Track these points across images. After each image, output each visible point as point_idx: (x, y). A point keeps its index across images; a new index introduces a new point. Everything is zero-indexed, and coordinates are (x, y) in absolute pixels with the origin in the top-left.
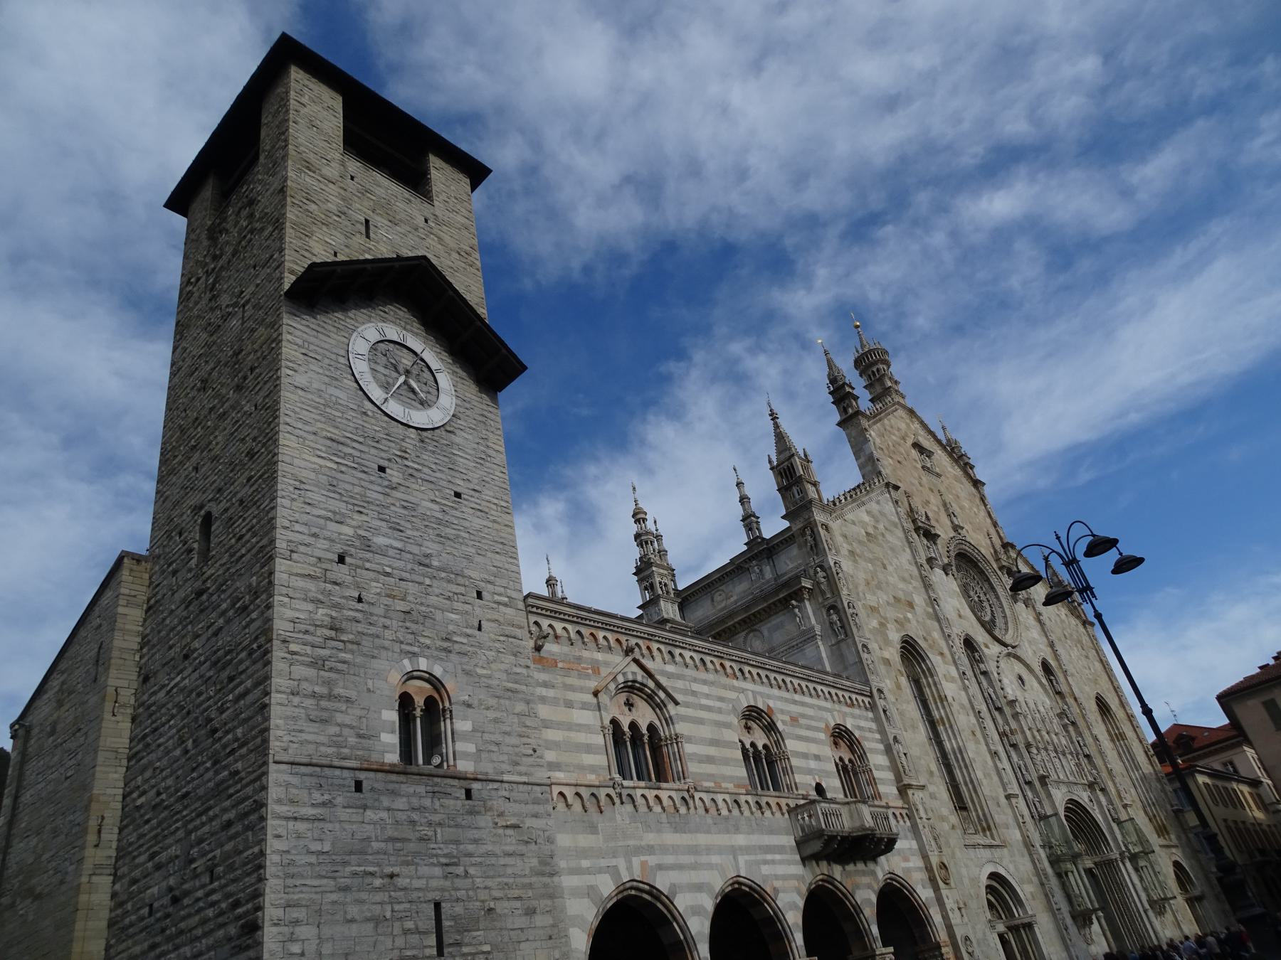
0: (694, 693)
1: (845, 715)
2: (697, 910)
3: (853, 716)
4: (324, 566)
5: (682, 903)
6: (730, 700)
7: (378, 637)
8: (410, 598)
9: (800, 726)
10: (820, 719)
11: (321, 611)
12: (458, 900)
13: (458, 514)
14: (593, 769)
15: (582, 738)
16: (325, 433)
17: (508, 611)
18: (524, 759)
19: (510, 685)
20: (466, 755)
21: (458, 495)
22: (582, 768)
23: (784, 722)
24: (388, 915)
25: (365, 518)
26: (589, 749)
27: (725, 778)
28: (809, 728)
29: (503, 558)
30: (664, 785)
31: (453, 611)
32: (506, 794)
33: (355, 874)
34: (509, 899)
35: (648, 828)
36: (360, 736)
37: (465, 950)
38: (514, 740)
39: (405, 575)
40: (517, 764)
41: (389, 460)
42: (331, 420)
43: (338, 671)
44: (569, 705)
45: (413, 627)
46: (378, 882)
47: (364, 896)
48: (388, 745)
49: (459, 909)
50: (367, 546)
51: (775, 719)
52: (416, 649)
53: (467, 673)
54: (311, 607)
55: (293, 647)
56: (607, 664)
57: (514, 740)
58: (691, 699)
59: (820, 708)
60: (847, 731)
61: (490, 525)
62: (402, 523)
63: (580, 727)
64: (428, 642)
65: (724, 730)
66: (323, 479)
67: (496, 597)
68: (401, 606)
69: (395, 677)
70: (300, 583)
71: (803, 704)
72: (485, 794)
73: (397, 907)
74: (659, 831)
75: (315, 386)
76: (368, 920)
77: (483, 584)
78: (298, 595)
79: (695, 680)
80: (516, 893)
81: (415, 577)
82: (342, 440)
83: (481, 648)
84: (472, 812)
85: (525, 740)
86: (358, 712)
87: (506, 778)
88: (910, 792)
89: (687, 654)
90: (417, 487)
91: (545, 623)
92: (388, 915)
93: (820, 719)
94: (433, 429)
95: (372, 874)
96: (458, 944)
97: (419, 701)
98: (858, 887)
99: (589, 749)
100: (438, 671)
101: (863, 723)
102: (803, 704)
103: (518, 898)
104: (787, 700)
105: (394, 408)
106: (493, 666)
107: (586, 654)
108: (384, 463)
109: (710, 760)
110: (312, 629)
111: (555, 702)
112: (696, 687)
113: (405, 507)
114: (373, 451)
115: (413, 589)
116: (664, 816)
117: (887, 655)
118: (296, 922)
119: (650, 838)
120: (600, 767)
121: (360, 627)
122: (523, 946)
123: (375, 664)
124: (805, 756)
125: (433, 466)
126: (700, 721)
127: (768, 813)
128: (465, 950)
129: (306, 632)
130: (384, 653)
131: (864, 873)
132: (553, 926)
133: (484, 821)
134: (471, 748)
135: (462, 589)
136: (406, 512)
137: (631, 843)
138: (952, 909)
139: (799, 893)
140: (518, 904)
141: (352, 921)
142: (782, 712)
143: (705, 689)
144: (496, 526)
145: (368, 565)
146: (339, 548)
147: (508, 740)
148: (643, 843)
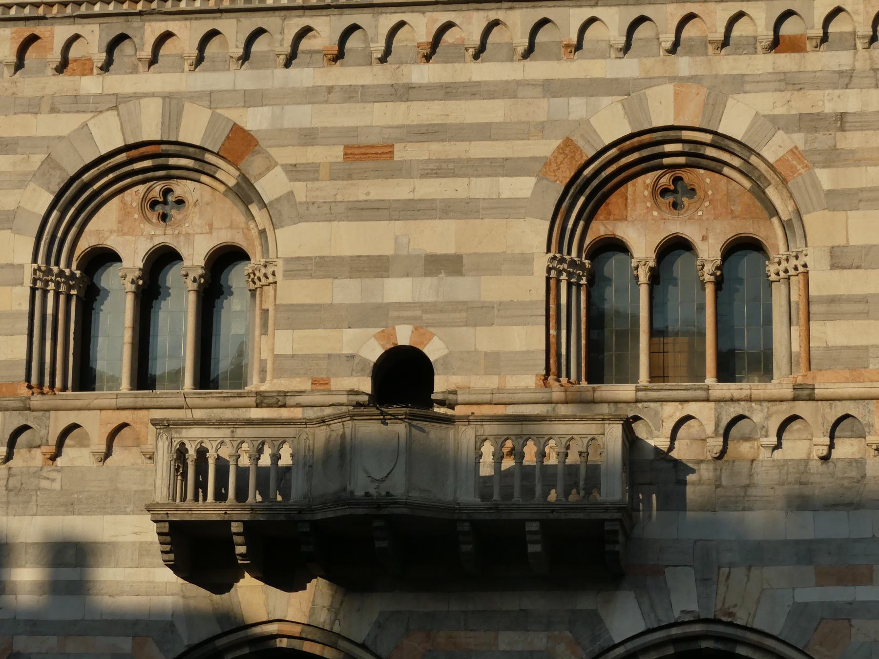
3: (788, 82)
6: (32, 143)
9: (403, 171)
10: (541, 129)
23: (294, 171)
51: (253, 165)
59: (551, 88)
93: (541, 129)
101: (851, 101)
102: (448, 91)
104: (353, 94)
124: (375, 267)
127: (75, 456)
131: (521, 621)
142: (308, 137)
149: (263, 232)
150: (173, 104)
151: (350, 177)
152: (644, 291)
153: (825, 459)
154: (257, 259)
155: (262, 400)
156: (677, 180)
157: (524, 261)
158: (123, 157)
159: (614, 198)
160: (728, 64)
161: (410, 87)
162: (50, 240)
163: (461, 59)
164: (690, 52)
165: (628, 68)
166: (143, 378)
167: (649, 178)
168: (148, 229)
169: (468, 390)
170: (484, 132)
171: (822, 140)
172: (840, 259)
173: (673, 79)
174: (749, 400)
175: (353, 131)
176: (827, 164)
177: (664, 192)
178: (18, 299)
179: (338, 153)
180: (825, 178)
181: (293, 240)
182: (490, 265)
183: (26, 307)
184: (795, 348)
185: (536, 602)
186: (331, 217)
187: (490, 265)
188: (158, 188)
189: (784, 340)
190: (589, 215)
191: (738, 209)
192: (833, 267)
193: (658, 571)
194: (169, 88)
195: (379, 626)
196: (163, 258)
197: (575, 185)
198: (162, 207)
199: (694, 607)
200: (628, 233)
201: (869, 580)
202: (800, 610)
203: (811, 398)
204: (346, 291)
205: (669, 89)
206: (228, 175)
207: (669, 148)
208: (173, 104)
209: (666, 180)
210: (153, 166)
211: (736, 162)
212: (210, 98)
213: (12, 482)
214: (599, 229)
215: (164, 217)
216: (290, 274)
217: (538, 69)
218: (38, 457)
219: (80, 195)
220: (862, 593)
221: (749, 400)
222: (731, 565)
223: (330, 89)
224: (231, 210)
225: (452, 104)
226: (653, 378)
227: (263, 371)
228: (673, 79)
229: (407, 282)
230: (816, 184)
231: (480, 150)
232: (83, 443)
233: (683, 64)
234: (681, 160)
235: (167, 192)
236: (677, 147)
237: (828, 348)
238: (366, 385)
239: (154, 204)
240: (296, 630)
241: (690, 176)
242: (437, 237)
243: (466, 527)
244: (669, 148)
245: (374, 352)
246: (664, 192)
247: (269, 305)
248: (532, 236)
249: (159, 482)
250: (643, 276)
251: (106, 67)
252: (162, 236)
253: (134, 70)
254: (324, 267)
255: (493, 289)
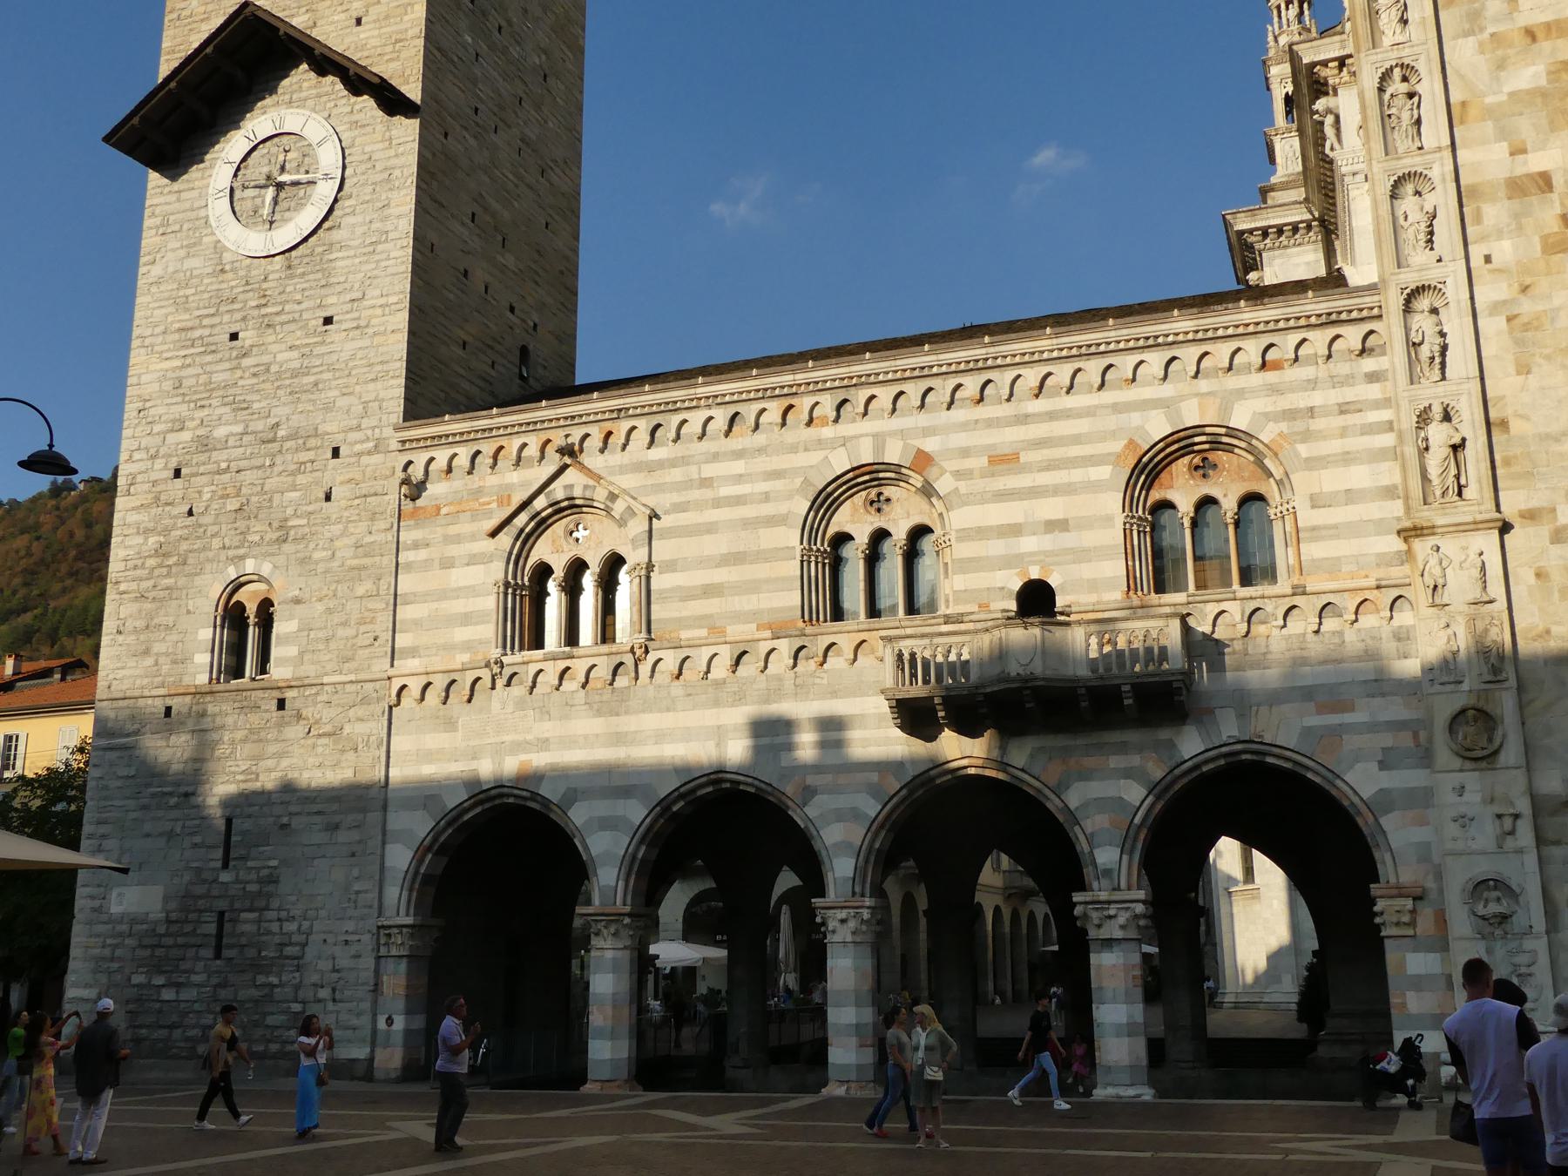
0: (706, 483)
1: (1241, 393)
2: (607, 824)
4: (158, 489)
5: (578, 816)
6: (795, 471)
7: (204, 549)
8: (244, 490)
10: (1113, 434)
11: (151, 540)
12: (249, 816)
13: (323, 349)
14: (467, 646)
15: (459, 606)
16: (177, 326)
17: (376, 459)
18: (360, 652)
19: (355, 562)
20: (283, 661)
21: (328, 321)
22: (450, 648)
23: (958, 475)
24: (178, 830)
25: (206, 411)
26: (466, 619)
27: (738, 617)
28: (1049, 466)
29: (379, 385)
30: (575, 651)
31: (294, 488)
32: (324, 697)
33: (153, 795)
34: (309, 814)
35: (544, 713)
36: (174, 662)
37: (250, 864)
38: (350, 632)
39: (243, 464)
40: (347, 660)
41: (244, 319)
42: (181, 304)
43: (162, 600)
44: (447, 564)
45: (241, 524)
46: (173, 801)
47: (160, 813)
48: (200, 665)
49: (247, 825)
50: (204, 445)
51: (932, 474)
52: (241, 551)
53: (303, 561)
54: (140, 540)
55: (123, 587)
56: (523, 485)
57: (350, 632)
58: (695, 494)
59: (1117, 408)
60: (1232, 432)
61: (366, 342)
62: (248, 398)
63: (457, 593)
64: (256, 538)
65: (761, 531)
66: (167, 386)
67: (358, 448)
68: (233, 505)
69: (216, 589)
70: (133, 518)
71: (1052, 416)
72: (298, 704)
73: (188, 823)
74: (565, 717)
75: (171, 269)
76: (161, 835)
77: (341, 436)
78: (131, 531)
79: (715, 457)
80: (316, 808)
81: (258, 462)
82: (189, 324)
83: (324, 524)
84: (281, 725)
85: (363, 629)
86: (175, 637)
87: (326, 680)
88: (1421, 547)
89: (696, 419)
90: (272, 338)
91: (420, 459)
92: (178, 830)
93: (1113, 434)
94: (305, 240)
95: (171, 794)
96: (244, 858)
97: (251, 609)
98: (1086, 775)
99: (466, 619)
100: (266, 569)
101: (1317, 399)
102: (1052, 416)
103: (319, 813)
104: (991, 423)
105: (255, 241)
106: (338, 544)
107: (492, 480)
108: (233, 330)
109: (709, 591)
110: (139, 562)
111: (426, 565)
112: (709, 470)
113: (254, 375)
114: (226, 318)
115: (248, 476)
116: (582, 692)
117: (1536, 162)
118: (103, 836)
119: (547, 729)
120: (481, 642)
121: (184, 546)
122: (316, 862)
123: (198, 581)
124: (1015, 530)
125: (298, 297)
126: (710, 528)
127: (835, 662)
128: (250, 864)
129: (135, 567)
130: (208, 567)
131: (1123, 748)
132: (360, 842)
133: (295, 731)
134: (292, 651)
135: (311, 455)
136: (255, 380)
137: (508, 738)
138: (1463, 820)
139: (874, 791)
140: (317, 819)
141: (148, 835)
142: (965, 452)
143: (739, 467)
144: (377, 340)
145: (202, 469)
146: (173, 464)
147: (341, 632)
148: (529, 737)
149: (941, 515)
150: (879, 439)
151: (993, 475)
152: (1188, 533)
153: (1317, 632)
154: (938, 531)
155: (948, 620)
156: (1204, 459)
157: (1109, 519)
158: (850, 475)
159: (1163, 475)
160: (1233, 382)
161: (1027, 416)
162: (810, 531)
163: (1059, 394)
164: (1207, 376)
165: (1167, 390)
166: (873, 611)
167: (1186, 460)
168: (869, 518)
169: (1079, 604)
170: (1077, 439)
171: (1300, 425)
172: (1316, 502)
173: (1197, 395)
174: (1263, 597)
175: (993, 446)
176: (1303, 441)
177: (1197, 468)
178: (793, 568)
179: (984, 461)
180: (1303, 450)
181: (959, 518)
182: (1086, 523)
183: (798, 573)
184: (1291, 561)
185: (1132, 736)
186: (983, 501)
187: (1086, 523)
188: (874, 492)
189: (1283, 557)
190: (1148, 486)
191: (1246, 474)
192: (1313, 507)
193: (1211, 711)
194: (876, 430)
195: (1032, 756)
196: (880, 536)
197: (1138, 468)
198: (878, 504)
199: (1235, 733)
200: (1173, 496)
201: (1352, 709)
202: (1307, 732)
203: (1304, 593)
204: (996, 547)
205: (1195, 401)
206: (917, 480)
207: (1197, 439)
208: (879, 439)
209: (1197, 460)
210: (869, 479)
211: (1243, 445)
212: (902, 434)
213: (799, 681)
214: (1156, 495)
215: (879, 510)
216: (959, 539)
217: (1107, 397)
218: (812, 664)
219: (826, 501)
220: (1348, 718)
221: (1263, 597)
222: (1259, 705)
223: (977, 421)
224: (921, 502)
225: (1055, 424)
226: (1198, 587)
227: (947, 601)
228: (1197, 395)
229: (1034, 538)
230: (1297, 455)
231: (1075, 451)
232: (839, 654)
233: (1203, 385)
234: (1206, 446)
235: (880, 494)
236: (1203, 438)
237: (1313, 560)
238: (1013, 606)
239: (872, 503)
240: (980, 762)
241: (1211, 456)
242: (1051, 508)
243: (1083, 691)
244: (1197, 439)
245: (1016, 585)
246: (1197, 468)
247: (947, 559)
248: (1112, 503)
249: (886, 674)
250: (1187, 523)
251: (836, 420)
252: (877, 522)
253: (854, 421)
254: (981, 533)
255: (1090, 538)
